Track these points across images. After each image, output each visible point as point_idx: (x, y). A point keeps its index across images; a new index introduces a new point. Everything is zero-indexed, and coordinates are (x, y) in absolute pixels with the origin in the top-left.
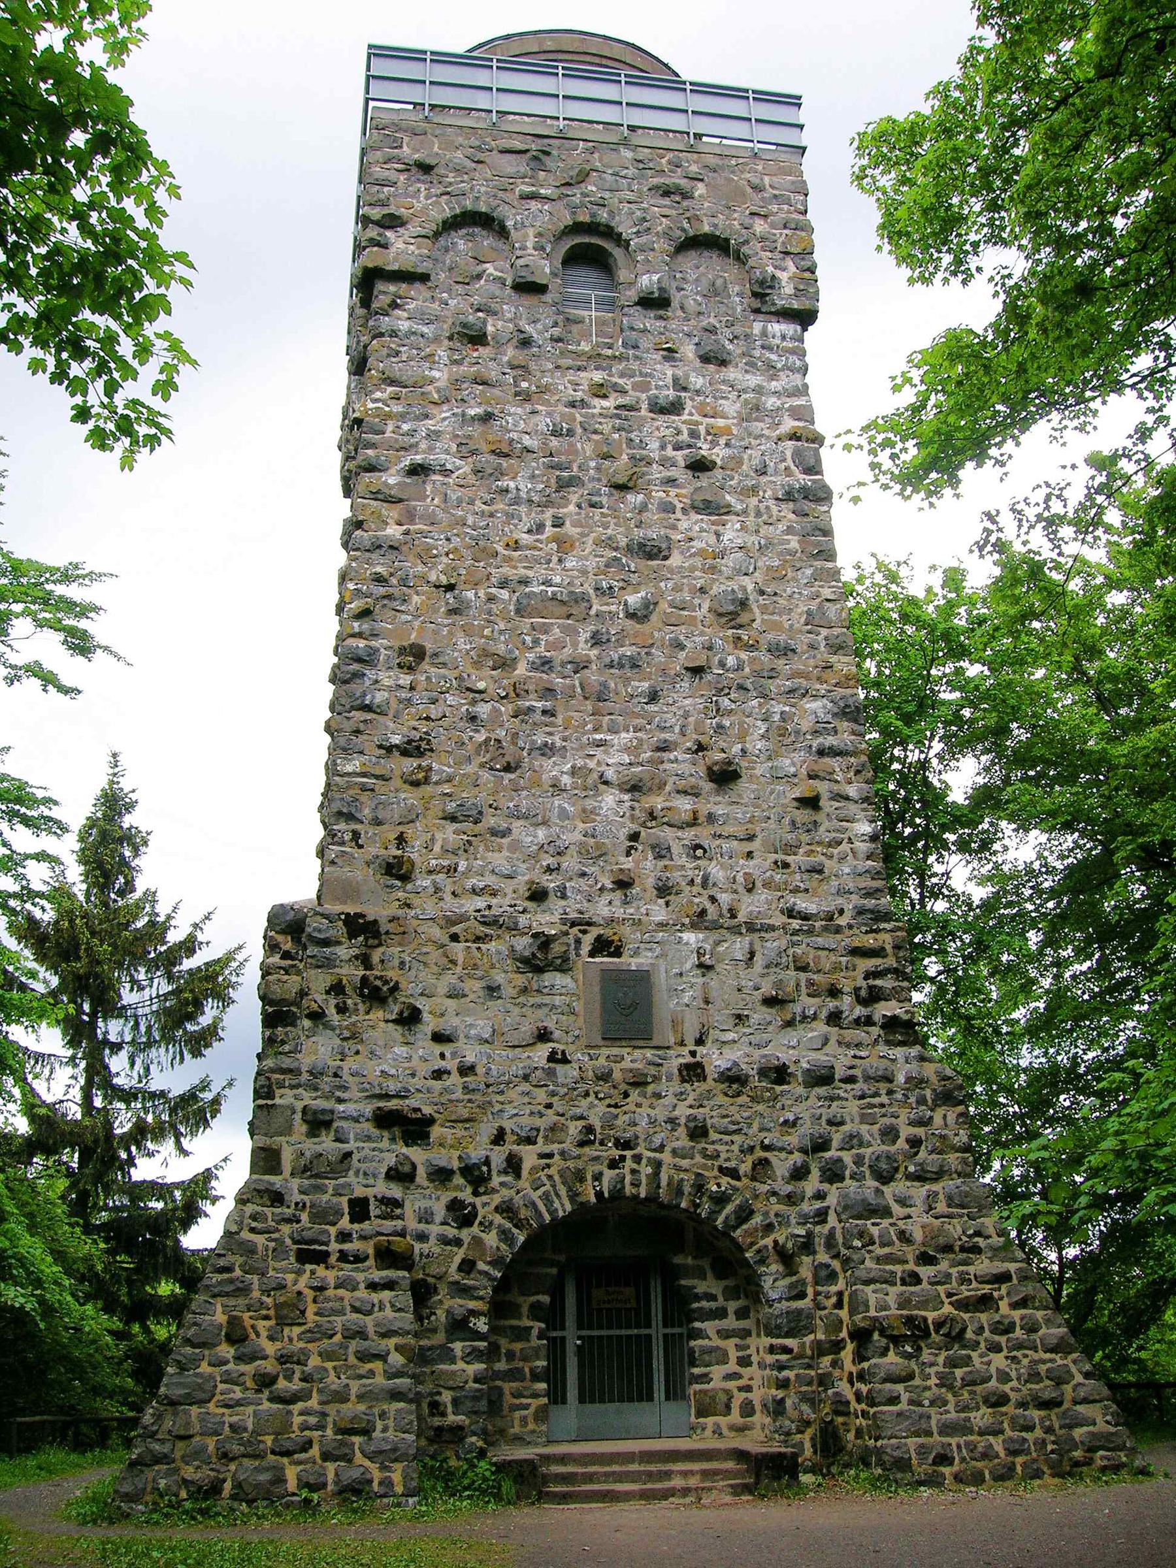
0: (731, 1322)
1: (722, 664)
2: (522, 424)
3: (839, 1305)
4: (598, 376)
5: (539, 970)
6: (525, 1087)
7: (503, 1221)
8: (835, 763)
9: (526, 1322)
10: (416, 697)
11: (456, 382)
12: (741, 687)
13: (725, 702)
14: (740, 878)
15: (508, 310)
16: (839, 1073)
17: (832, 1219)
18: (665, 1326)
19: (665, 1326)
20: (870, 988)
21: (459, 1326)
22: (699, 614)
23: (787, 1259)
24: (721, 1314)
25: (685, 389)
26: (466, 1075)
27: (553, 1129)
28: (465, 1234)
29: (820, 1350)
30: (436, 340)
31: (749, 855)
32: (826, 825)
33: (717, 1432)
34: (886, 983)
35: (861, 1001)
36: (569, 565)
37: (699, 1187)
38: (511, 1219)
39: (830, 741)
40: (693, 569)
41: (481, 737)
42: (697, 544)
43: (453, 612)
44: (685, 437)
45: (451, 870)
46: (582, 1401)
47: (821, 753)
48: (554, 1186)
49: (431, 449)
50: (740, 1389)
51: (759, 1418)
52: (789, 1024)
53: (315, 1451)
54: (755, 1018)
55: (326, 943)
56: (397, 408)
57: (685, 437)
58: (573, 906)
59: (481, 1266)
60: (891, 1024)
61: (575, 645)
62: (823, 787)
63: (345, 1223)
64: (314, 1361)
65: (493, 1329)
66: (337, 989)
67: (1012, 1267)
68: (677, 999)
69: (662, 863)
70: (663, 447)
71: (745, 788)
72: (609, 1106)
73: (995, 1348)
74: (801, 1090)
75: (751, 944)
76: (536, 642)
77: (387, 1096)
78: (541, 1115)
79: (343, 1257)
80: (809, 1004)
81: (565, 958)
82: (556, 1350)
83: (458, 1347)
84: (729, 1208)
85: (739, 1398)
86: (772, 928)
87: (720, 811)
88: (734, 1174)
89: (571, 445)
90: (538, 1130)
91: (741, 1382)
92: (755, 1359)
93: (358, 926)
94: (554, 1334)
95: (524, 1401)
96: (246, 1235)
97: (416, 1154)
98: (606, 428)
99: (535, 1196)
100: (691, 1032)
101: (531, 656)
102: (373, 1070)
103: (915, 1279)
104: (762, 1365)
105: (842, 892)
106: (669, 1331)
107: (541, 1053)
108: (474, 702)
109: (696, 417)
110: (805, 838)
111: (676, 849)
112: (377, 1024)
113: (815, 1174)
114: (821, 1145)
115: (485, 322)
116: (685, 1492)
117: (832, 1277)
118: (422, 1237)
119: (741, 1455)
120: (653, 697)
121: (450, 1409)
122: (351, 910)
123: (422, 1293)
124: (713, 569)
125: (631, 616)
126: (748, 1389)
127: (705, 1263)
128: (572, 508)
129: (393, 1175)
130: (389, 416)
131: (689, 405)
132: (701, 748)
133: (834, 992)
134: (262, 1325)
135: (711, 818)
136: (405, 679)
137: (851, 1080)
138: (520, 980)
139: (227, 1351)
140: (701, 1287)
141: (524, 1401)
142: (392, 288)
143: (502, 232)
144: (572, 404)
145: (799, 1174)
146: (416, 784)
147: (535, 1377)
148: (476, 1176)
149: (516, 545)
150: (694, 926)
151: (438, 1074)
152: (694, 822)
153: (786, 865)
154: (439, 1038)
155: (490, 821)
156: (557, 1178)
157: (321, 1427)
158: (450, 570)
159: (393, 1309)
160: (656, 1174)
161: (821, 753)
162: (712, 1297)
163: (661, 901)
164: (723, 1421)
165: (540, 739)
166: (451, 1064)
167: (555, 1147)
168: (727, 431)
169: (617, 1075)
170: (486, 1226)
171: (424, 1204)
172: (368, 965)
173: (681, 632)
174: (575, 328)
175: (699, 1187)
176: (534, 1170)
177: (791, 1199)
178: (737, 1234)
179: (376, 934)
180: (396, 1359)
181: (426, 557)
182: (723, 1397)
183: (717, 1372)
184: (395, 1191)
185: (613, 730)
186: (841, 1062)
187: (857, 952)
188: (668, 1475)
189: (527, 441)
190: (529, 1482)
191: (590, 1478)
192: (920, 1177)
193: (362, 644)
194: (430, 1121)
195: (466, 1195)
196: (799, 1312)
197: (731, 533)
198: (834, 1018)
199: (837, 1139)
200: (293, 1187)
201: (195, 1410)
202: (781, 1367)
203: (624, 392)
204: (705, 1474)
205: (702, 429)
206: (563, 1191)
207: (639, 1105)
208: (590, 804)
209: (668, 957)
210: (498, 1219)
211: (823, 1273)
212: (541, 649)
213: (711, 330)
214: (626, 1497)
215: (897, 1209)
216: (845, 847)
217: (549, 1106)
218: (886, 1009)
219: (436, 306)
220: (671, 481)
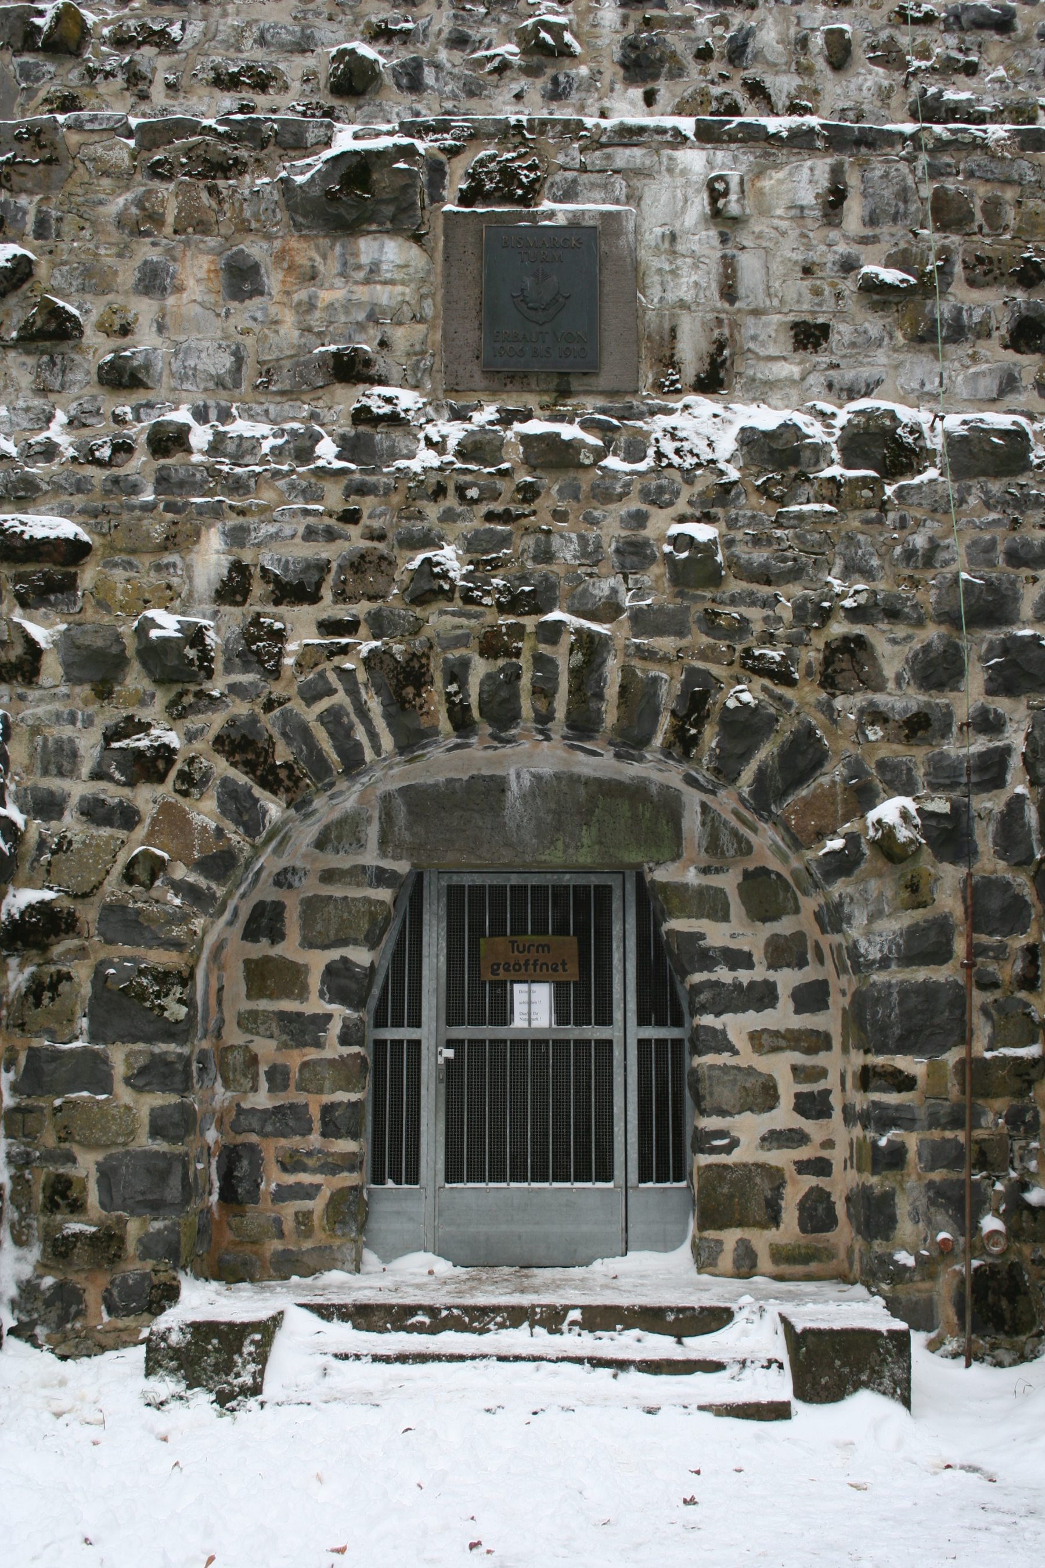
0: (783, 1016)
7: (233, 773)
9: (315, 1005)
14: (818, 41)
18: (643, 1020)
19: (643, 1020)
24: (762, 996)
26: (166, 453)
27: (359, 564)
38: (250, 768)
46: (452, 1175)
48: (353, 691)
50: (803, 1167)
54: (842, 331)
69: (636, 16)
72: (490, 517)
75: (837, 172)
78: (331, 535)
84: (766, 752)
85: (796, 1191)
90: (323, 567)
91: (804, 1153)
92: (836, 1101)
94: (390, 1034)
95: (305, 1178)
99: (310, 714)
104: (849, 1115)
106: (652, 1033)
114: (991, 607)
117: (1013, 915)
121: (93, 1197)
126: (820, 1167)
141: (305, 1178)
145: (938, 670)
154: (122, 377)
156: (362, 676)
162: (739, 959)
163: (637, 93)
164: (761, 1240)
166: (138, 432)
167: (362, 608)
170: (191, 782)
176: (308, 658)
182: (763, 1185)
183: (749, 1128)
196: (928, 991)
202: (884, 1119)
206: (374, 705)
207: (560, 516)
210: (221, 767)
211: (994, 903)
217: (351, 517)
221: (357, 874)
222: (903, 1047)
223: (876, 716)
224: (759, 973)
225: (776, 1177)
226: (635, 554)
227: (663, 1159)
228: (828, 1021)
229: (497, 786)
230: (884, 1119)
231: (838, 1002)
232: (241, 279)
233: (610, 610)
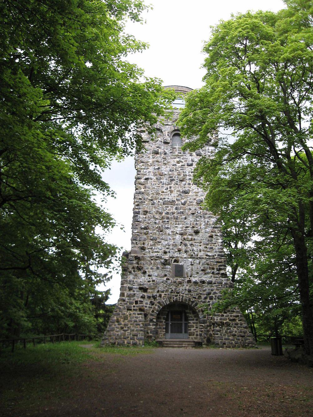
1: (197, 212)
2: (165, 170)
3: (211, 319)
4: (178, 159)
5: (165, 265)
6: (163, 284)
8: (216, 229)
10: (146, 219)
12: (201, 217)
13: (198, 219)
15: (163, 147)
21: (151, 320)
22: (194, 203)
23: (203, 311)
24: (193, 320)
28: (153, 306)
29: (208, 326)
30: (150, 154)
31: (200, 246)
32: (214, 240)
33: (192, 338)
35: (217, 270)
36: (172, 195)
37: (190, 300)
41: (157, 226)
42: (194, 191)
43: (152, 204)
45: (152, 248)
49: (149, 175)
51: (199, 337)
52: (205, 274)
53: (129, 338)
55: (132, 261)
56: (143, 167)
58: (171, 254)
59: (155, 311)
60: (223, 274)
62: (214, 234)
63: (134, 304)
64: (129, 325)
66: (133, 268)
67: (239, 314)
68: (187, 269)
71: (200, 234)
73: (235, 327)
76: (166, 209)
77: (141, 285)
79: (134, 310)
80: (209, 271)
81: (169, 263)
82: (167, 325)
83: (151, 324)
84: (194, 303)
85: (196, 333)
86: (203, 258)
87: (196, 238)
88: (195, 298)
93: (137, 258)
96: (119, 306)
97: (145, 294)
98: (179, 170)
99: (164, 301)
100: (189, 275)
101: (165, 212)
102: (139, 281)
103: (223, 316)
105: (216, 252)
107: (165, 279)
108: (156, 220)
111: (188, 245)
112: (140, 273)
114: (209, 294)
116: (185, 347)
118: (146, 307)
119: (194, 342)
120: (185, 218)
122: (136, 255)
123: (146, 315)
124: (197, 195)
125: (182, 204)
126: (197, 332)
127: (191, 312)
128: (173, 185)
129: (142, 297)
130: (142, 169)
133: (213, 269)
134: (122, 320)
135: (194, 239)
136: (145, 216)
137: (215, 283)
138: (162, 267)
139: (116, 324)
140: (190, 315)
143: (162, 132)
144: (173, 165)
145: (206, 298)
146: (146, 234)
147: (163, 328)
148: (154, 298)
149: (163, 192)
150: (191, 258)
151: (149, 281)
152: (191, 240)
153: (206, 247)
154: (149, 276)
155: (158, 240)
157: (130, 335)
159: (141, 318)
160: (183, 298)
161: (214, 228)
164: (193, 337)
165: (166, 226)
169: (177, 282)
170: (156, 305)
171: (146, 302)
172: (138, 264)
173: (191, 207)
174: (175, 150)
175: (190, 300)
176: (164, 297)
177: (204, 302)
178: (195, 307)
179: (140, 259)
180: (141, 325)
181: (148, 194)
183: (192, 329)
184: (142, 300)
185: (179, 224)
186: (214, 280)
187: (217, 262)
188: (182, 344)
189: (166, 173)
190: (161, 344)
191: (170, 344)
193: (137, 210)
194: (147, 289)
195: (153, 300)
198: (213, 273)
199: (212, 293)
200: (127, 299)
201: (112, 332)
203: (182, 162)
204: (188, 344)
208: (174, 237)
209: (186, 263)
210: (158, 304)
212: (167, 211)
214: (176, 347)
216: (217, 244)
218: (222, 272)
219: (150, 147)
222: (203, 323)
224: (193, 318)
225: (194, 332)
227: (186, 332)
230: (201, 328)
232: (158, 268)
233: (183, 294)
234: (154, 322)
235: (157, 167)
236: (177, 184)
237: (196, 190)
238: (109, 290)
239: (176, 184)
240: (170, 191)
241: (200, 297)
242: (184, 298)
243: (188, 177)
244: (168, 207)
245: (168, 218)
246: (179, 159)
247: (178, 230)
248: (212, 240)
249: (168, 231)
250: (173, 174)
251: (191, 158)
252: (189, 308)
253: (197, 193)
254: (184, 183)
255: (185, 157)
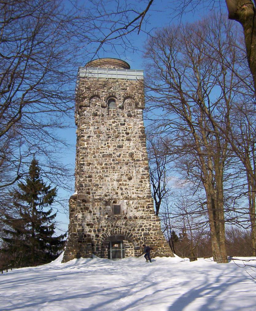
2: (103, 128)
4: (113, 120)
8: (145, 176)
11: (93, 123)
12: (132, 166)
16: (144, 217)
17: (143, 236)
20: (148, 207)
24: (129, 247)
25: (125, 121)
30: (91, 116)
31: (133, 189)
34: (150, 206)
35: (147, 208)
36: (109, 150)
39: (144, 173)
40: (126, 149)
41: (98, 175)
44: (125, 129)
47: (143, 175)
49: (90, 133)
54: (133, 211)
56: (86, 127)
57: (125, 129)
61: (110, 161)
62: (143, 180)
65: (101, 250)
68: (124, 208)
70: (122, 131)
71: (132, 181)
74: (139, 220)
76: (105, 161)
80: (140, 209)
89: (110, 131)
100: (125, 212)
109: (127, 126)
110: (140, 187)
111: (124, 189)
113: (141, 230)
115: (97, 113)
117: (142, 243)
124: (129, 149)
128: (110, 141)
130: (85, 129)
131: (126, 124)
132: (127, 175)
138: (104, 207)
142: (84, 108)
144: (109, 125)
145: (139, 230)
149: (102, 147)
150: (126, 199)
153: (138, 191)
158: (94, 152)
162: (128, 245)
165: (106, 175)
168: (131, 128)
173: (124, 159)
185: (115, 173)
192: (154, 230)
197: (132, 144)
198: (143, 210)
199: (143, 225)
205: (128, 128)
208: (112, 183)
210: (102, 237)
213: (129, 111)
215: (151, 235)
216: (146, 188)
220: (123, 136)
221: (107, 241)
223: (135, 233)
224: (129, 246)
226: (123, 224)
228: (133, 248)
229: (115, 236)
231: (133, 248)
234: (100, 251)
235: (96, 127)
236: (113, 141)
237: (128, 145)
238: (53, 224)
239: (112, 140)
240: (107, 146)
241: (134, 230)
242: (122, 231)
243: (121, 135)
244: (106, 159)
245: (107, 168)
246: (114, 120)
247: (116, 176)
248: (142, 185)
249: (107, 179)
250: (110, 132)
251: (123, 119)
252: (125, 238)
253: (129, 147)
254: (118, 139)
255: (118, 118)
